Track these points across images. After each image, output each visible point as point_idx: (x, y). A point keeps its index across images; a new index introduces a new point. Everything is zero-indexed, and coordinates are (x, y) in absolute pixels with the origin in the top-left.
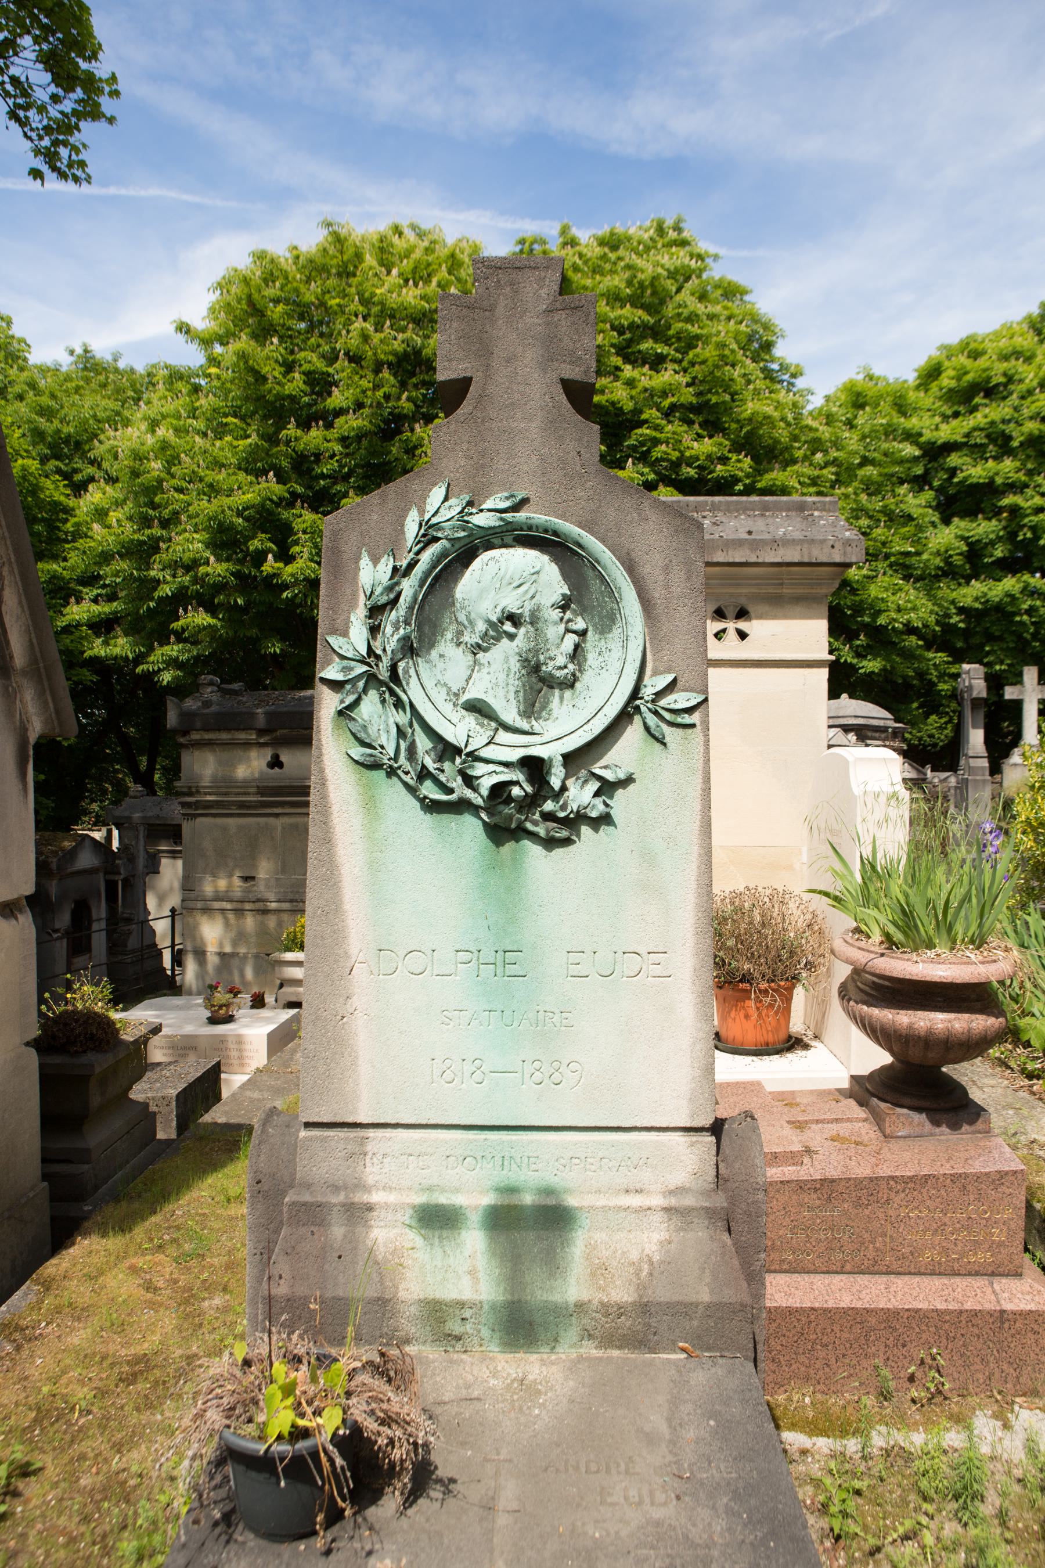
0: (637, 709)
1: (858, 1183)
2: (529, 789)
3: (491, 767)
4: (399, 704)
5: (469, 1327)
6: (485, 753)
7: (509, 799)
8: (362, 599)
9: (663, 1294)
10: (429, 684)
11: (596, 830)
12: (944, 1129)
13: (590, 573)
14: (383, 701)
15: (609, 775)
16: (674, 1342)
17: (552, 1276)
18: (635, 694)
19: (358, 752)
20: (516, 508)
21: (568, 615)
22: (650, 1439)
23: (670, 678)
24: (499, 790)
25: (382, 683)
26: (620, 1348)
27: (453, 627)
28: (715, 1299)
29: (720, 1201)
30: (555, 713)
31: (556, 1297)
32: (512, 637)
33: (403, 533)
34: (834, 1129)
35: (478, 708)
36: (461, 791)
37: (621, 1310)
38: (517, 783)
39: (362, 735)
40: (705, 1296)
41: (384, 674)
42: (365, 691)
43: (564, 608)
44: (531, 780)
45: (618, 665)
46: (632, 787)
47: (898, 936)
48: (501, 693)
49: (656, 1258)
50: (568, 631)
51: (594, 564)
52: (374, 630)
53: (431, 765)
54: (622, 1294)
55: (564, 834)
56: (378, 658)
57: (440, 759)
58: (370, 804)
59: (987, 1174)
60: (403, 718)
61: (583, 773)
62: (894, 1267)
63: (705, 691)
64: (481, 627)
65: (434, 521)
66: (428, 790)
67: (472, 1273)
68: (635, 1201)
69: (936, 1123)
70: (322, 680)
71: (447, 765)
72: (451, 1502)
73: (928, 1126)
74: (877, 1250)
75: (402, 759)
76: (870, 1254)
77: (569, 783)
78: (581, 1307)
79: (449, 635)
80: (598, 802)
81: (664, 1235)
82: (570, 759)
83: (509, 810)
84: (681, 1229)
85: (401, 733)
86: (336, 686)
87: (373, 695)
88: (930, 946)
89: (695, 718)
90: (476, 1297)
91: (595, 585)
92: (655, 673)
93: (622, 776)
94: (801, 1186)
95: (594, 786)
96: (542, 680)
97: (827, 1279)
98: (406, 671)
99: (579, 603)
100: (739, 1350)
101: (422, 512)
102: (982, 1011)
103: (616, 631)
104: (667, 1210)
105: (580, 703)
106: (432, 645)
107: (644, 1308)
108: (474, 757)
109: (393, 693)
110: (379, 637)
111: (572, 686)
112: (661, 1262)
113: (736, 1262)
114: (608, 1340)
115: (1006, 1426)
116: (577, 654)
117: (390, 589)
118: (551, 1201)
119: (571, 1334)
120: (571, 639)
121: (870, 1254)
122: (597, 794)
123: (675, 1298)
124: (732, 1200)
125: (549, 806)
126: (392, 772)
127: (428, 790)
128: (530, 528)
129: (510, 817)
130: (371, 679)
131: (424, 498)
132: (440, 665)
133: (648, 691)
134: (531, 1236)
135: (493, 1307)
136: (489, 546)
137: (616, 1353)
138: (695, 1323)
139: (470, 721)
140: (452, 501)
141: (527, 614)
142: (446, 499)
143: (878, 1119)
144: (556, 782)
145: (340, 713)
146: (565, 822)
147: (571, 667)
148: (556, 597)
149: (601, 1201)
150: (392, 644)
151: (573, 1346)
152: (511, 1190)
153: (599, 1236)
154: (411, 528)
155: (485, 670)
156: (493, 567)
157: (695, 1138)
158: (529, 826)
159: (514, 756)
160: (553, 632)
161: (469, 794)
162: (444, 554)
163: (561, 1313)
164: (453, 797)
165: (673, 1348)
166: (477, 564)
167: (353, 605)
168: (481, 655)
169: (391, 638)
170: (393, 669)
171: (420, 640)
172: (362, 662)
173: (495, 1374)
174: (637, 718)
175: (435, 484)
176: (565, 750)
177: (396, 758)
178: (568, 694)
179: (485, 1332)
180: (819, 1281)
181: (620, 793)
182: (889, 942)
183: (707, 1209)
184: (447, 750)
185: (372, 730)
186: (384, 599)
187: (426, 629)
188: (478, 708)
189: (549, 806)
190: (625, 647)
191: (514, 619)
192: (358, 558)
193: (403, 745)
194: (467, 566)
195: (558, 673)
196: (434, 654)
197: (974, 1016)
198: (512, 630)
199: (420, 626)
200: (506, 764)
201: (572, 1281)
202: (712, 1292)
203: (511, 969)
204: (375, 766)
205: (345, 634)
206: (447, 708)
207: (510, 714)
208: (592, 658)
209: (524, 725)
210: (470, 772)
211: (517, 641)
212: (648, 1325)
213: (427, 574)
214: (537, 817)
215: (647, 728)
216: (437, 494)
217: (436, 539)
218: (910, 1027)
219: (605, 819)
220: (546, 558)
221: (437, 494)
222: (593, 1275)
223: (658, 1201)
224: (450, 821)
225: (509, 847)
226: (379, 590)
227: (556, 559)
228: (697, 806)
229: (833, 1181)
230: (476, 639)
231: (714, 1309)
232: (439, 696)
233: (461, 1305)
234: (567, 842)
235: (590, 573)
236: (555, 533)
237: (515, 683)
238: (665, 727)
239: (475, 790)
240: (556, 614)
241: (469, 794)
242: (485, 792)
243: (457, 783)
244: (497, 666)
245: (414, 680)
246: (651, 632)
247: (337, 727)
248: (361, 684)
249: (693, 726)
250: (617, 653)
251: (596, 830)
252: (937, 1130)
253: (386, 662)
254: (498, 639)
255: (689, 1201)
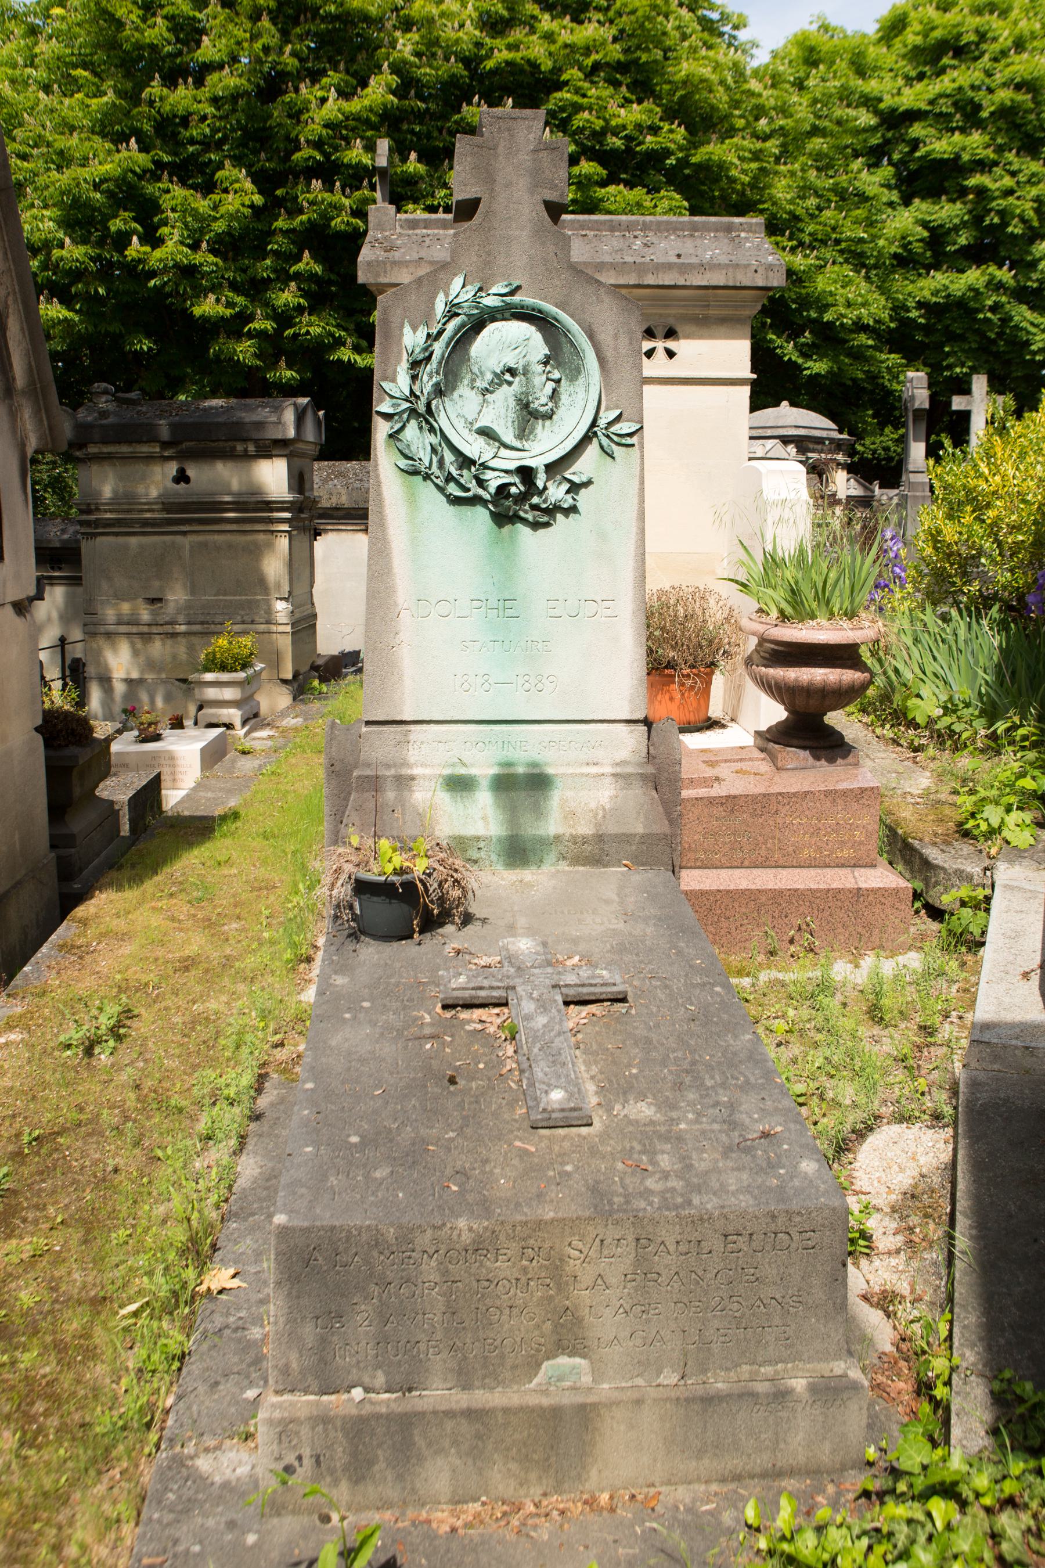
0: (595, 433)
1: (753, 799)
2: (522, 488)
3: (497, 473)
4: (432, 430)
5: (483, 854)
6: (492, 464)
7: (509, 495)
8: (405, 356)
9: (612, 828)
10: (452, 416)
11: (567, 517)
12: (823, 762)
13: (563, 339)
14: (421, 428)
15: (576, 479)
16: (620, 861)
17: (538, 819)
18: (594, 424)
19: (403, 463)
20: (512, 293)
21: (548, 368)
22: (607, 902)
23: (617, 412)
24: (502, 489)
25: (419, 415)
26: (583, 865)
27: (469, 376)
28: (647, 831)
29: (650, 769)
30: (539, 436)
31: (541, 832)
32: (510, 384)
33: (433, 309)
34: (739, 765)
35: (486, 433)
36: (475, 490)
37: (585, 840)
38: (515, 484)
39: (406, 451)
40: (640, 829)
41: (422, 408)
42: (408, 420)
43: (546, 363)
44: (523, 482)
45: (582, 404)
46: (591, 487)
47: (789, 610)
48: (502, 422)
49: (607, 807)
50: (548, 379)
51: (566, 333)
52: (414, 378)
53: (455, 473)
54: (585, 829)
55: (545, 519)
56: (417, 397)
57: (460, 468)
58: (412, 499)
59: (852, 790)
60: (434, 440)
61: (558, 477)
62: (781, 862)
63: (641, 421)
64: (489, 376)
65: (456, 301)
66: (453, 489)
67: (484, 818)
68: (593, 770)
69: (817, 758)
70: (378, 413)
71: (465, 472)
72: (486, 926)
73: (811, 760)
74: (768, 849)
75: (435, 468)
76: (763, 852)
77: (549, 484)
78: (558, 838)
79: (466, 382)
80: (569, 497)
81: (613, 792)
82: (551, 468)
83: (508, 503)
84: (622, 789)
85: (434, 450)
86: (388, 417)
87: (413, 424)
88: (813, 617)
89: (634, 440)
90: (488, 833)
91: (567, 347)
92: (608, 409)
93: (585, 480)
94: (711, 801)
95: (566, 486)
96: (530, 413)
97: (730, 871)
98: (437, 407)
99: (556, 360)
100: (663, 865)
101: (447, 295)
102: (850, 667)
103: (581, 380)
104: (614, 775)
105: (556, 429)
106: (454, 389)
107: (600, 838)
108: (484, 466)
109: (428, 422)
110: (418, 383)
111: (551, 418)
112: (611, 809)
113: (661, 808)
114: (577, 860)
115: (857, 966)
116: (554, 395)
117: (426, 349)
118: (536, 771)
119: (552, 857)
120: (551, 385)
121: (763, 852)
122: (568, 492)
123: (620, 831)
124: (658, 769)
125: (535, 500)
126: (427, 477)
127: (453, 489)
128: (522, 307)
129: (509, 508)
130: (413, 412)
131: (448, 284)
132: (460, 403)
133: (602, 422)
134: (523, 794)
135: (499, 840)
136: (494, 320)
137: (581, 868)
138: (634, 848)
139: (481, 441)
140: (468, 288)
141: (521, 368)
142: (464, 286)
143: (773, 758)
144: (540, 484)
145: (391, 436)
146: (547, 511)
147: (550, 404)
148: (541, 357)
149: (570, 771)
150: (428, 388)
151: (553, 865)
152: (509, 764)
153: (569, 794)
154: (440, 307)
155: (491, 406)
156: (497, 336)
157: (633, 727)
158: (522, 514)
159: (513, 465)
160: (538, 380)
161: (481, 492)
162: (463, 325)
163: (545, 843)
164: (470, 494)
165: (619, 864)
166: (485, 332)
167: (399, 361)
168: (488, 396)
169: (427, 384)
170: (428, 405)
171: (446, 386)
172: (407, 400)
173: (503, 879)
174: (595, 440)
175: (455, 275)
176: (547, 462)
177: (430, 468)
178: (548, 423)
179: (494, 857)
180: (724, 873)
181: (583, 491)
182: (783, 616)
183: (641, 774)
184: (466, 462)
185: (413, 448)
186: (421, 356)
187: (450, 377)
188: (486, 433)
189: (535, 500)
190: (587, 391)
191: (512, 371)
192: (402, 326)
193: (435, 459)
194: (478, 332)
195: (542, 409)
196: (456, 394)
197: (844, 671)
198: (510, 379)
199: (446, 375)
200: (506, 472)
201: (552, 822)
202: (645, 827)
203: (509, 613)
204: (415, 473)
205: (394, 380)
206: (465, 433)
207: (508, 438)
208: (564, 398)
209: (519, 446)
210: (482, 477)
211: (513, 386)
212: (602, 849)
213: (451, 339)
214: (527, 507)
215: (602, 447)
216: (458, 281)
217: (458, 315)
218: (796, 680)
219: (573, 509)
220: (533, 328)
221: (458, 281)
222: (565, 818)
223: (608, 770)
224: (467, 511)
225: (508, 528)
226: (417, 350)
227: (540, 329)
228: (636, 500)
229: (735, 797)
230: (485, 385)
231: (646, 838)
232: (460, 424)
233: (478, 839)
234: (547, 525)
235: (563, 339)
236: (540, 311)
237: (512, 416)
238: (613, 446)
239: (485, 489)
240: (540, 368)
241: (481, 492)
242: (492, 490)
243: (473, 485)
244: (500, 403)
245: (442, 413)
246: (605, 380)
247: (388, 446)
248: (405, 416)
249: (633, 445)
250: (581, 394)
251: (567, 517)
252: (818, 763)
253: (423, 400)
254: (500, 385)
255: (630, 770)
